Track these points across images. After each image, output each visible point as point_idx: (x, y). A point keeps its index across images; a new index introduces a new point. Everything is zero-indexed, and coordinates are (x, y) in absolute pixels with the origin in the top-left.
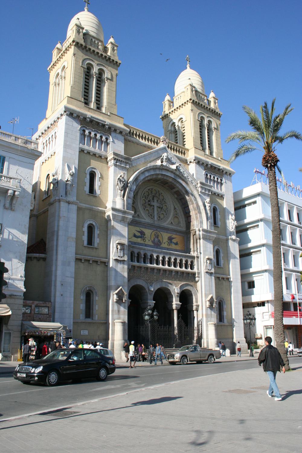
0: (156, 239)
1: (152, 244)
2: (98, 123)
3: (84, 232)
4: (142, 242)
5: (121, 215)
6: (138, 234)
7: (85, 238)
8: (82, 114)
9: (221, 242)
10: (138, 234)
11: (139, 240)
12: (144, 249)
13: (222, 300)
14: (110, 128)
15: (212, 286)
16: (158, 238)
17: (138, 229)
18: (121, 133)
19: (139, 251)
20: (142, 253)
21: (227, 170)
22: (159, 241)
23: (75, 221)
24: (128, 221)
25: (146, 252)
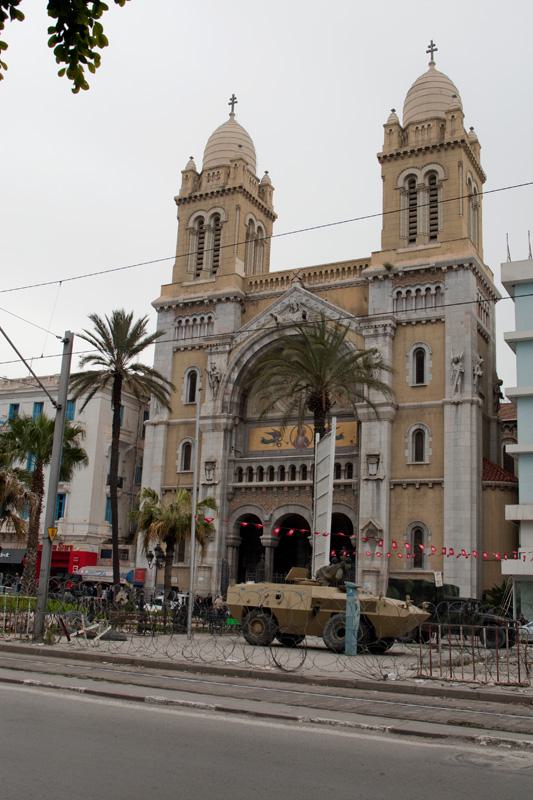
0: (300, 439)
1: (293, 447)
2: (193, 303)
3: (177, 455)
4: (276, 448)
5: (210, 421)
6: (271, 437)
7: (179, 463)
8: (173, 302)
9: (429, 414)
10: (271, 437)
11: (271, 446)
12: (256, 461)
13: (421, 525)
14: (211, 301)
15: (379, 503)
16: (303, 435)
17: (270, 430)
18: (228, 299)
19: (249, 465)
20: (254, 466)
21: (448, 262)
22: (306, 440)
23: (162, 445)
24: (223, 427)
25: (261, 464)
